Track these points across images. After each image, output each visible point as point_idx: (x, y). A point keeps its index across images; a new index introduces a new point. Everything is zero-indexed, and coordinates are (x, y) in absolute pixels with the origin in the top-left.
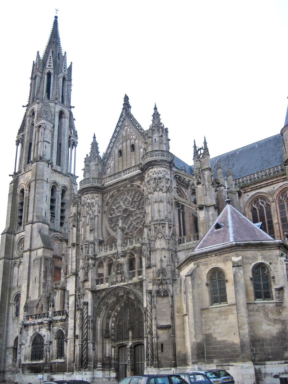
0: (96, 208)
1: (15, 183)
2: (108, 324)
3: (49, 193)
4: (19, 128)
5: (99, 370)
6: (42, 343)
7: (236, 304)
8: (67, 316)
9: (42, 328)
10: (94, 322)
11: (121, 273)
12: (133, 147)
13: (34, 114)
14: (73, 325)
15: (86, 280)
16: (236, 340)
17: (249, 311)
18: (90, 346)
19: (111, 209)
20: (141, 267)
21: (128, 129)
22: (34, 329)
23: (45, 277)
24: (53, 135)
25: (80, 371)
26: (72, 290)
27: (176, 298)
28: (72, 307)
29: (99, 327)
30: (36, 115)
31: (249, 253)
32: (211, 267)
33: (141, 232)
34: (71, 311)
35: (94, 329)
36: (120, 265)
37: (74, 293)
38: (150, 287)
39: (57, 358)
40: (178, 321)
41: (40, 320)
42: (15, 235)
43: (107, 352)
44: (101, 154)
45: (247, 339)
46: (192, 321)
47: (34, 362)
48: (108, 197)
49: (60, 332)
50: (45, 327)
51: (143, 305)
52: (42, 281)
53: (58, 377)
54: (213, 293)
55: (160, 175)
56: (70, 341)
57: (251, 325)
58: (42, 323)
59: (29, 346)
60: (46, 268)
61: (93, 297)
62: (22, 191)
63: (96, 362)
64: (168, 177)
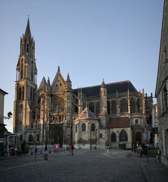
0: (50, 101)
1: (18, 85)
3: (30, 91)
4: (17, 64)
6: (32, 137)
7: (88, 132)
8: (40, 130)
10: (49, 132)
12: (61, 85)
13: (23, 60)
14: (42, 133)
15: (47, 121)
16: (87, 139)
17: (90, 133)
18: (48, 139)
19: (54, 101)
20: (63, 119)
21: (59, 78)
23: (31, 118)
24: (30, 70)
27: (73, 129)
29: (50, 134)
30: (24, 61)
31: (91, 121)
32: (83, 123)
33: (63, 110)
35: (49, 134)
36: (57, 118)
38: (66, 125)
40: (73, 134)
41: (31, 131)
42: (19, 103)
44: (51, 84)
45: (89, 139)
46: (78, 135)
47: (30, 142)
48: (53, 98)
49: (38, 134)
51: (63, 129)
52: (30, 119)
54: (82, 129)
55: (69, 95)
57: (90, 137)
60: (31, 115)
61: (49, 126)
62: (20, 88)
63: (50, 143)
64: (71, 96)
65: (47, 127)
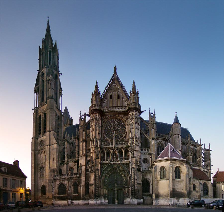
2: (105, 180)
5: (103, 199)
9: (64, 180)
11: (115, 157)
22: (59, 181)
25: (95, 199)
26: (84, 163)
28: (84, 171)
29: (102, 181)
34: (83, 173)
37: (85, 165)
39: (74, 194)
43: (104, 192)
50: (66, 180)
53: (76, 202)
56: (83, 187)
58: (64, 178)
59: (57, 189)
61: (101, 166)
65: (97, 168)
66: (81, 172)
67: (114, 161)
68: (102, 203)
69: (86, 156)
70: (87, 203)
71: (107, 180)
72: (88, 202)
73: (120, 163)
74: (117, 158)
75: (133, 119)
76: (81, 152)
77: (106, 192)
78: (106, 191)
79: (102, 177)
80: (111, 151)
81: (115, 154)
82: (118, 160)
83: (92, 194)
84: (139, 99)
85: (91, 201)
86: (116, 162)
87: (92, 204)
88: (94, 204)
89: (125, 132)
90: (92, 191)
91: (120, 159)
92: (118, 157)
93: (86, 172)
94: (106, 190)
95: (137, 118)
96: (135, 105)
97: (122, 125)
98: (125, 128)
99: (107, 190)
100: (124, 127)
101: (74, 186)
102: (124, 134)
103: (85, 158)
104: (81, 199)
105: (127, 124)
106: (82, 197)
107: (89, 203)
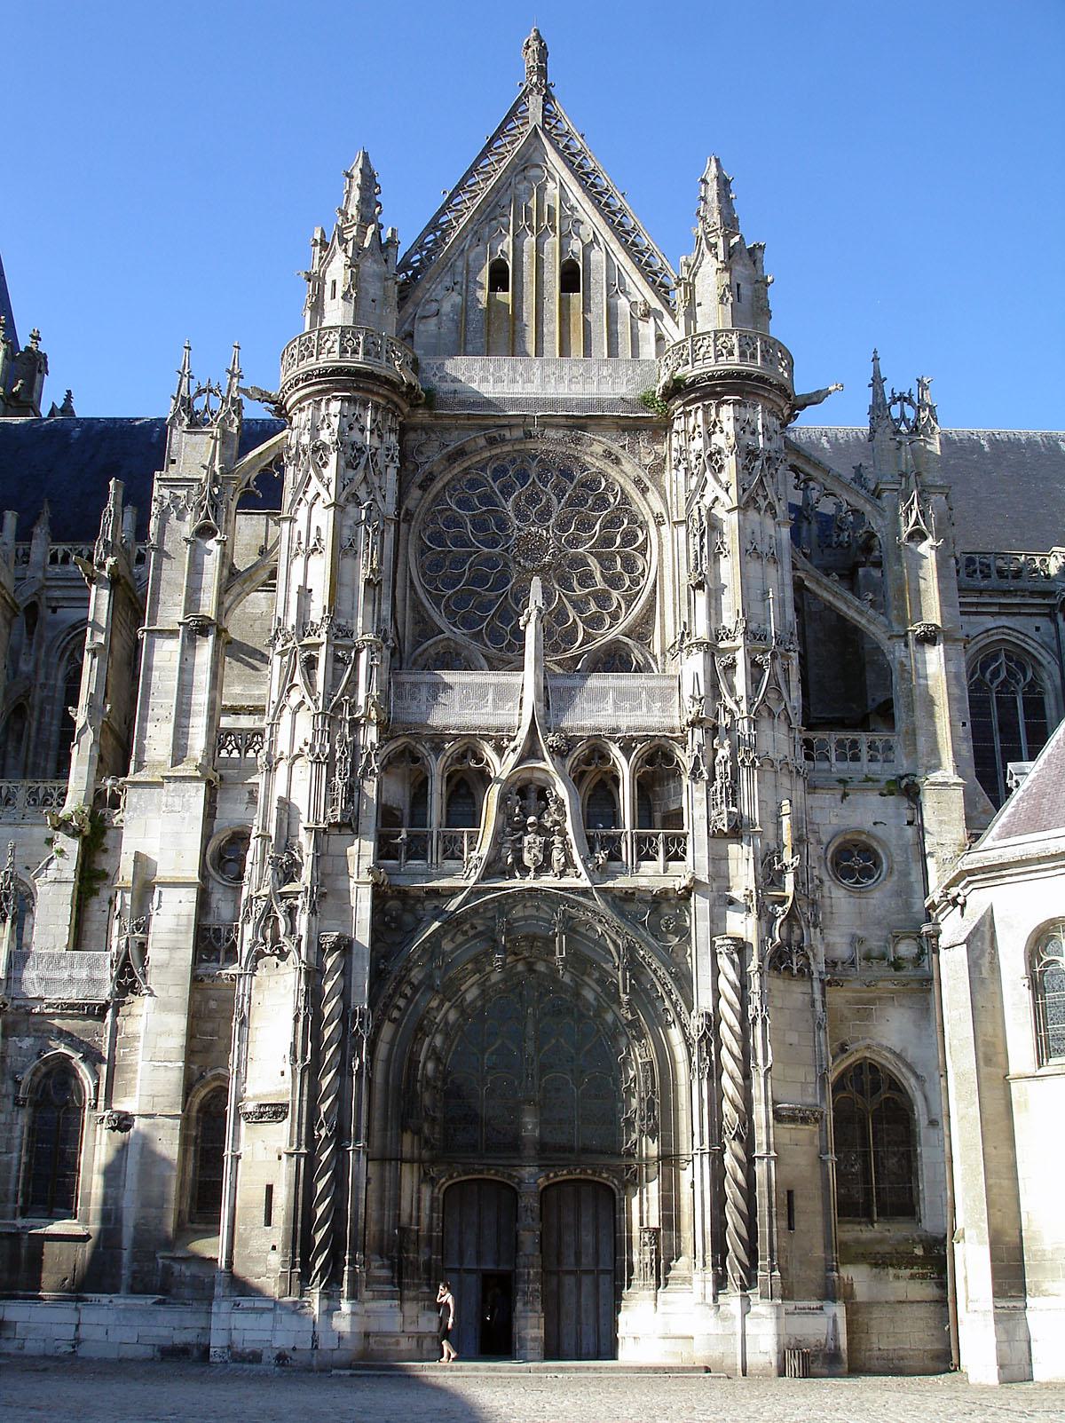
2: (413, 1063)
11: (541, 830)
26: (180, 854)
28: (173, 949)
29: (379, 1078)
37: (194, 876)
43: (405, 1204)
66: (143, 947)
67: (525, 871)
68: (372, 1340)
69: (209, 783)
70: (180, 1338)
71: (430, 1066)
72: (206, 1330)
73: (585, 892)
74: (563, 833)
75: (721, 467)
76: (157, 739)
77: (426, 1203)
78: (426, 1192)
79: (387, 1030)
80: (501, 767)
81: (533, 796)
82: (569, 862)
83: (268, 1222)
84: (772, 294)
85: (239, 1320)
86: (548, 881)
87: (255, 1357)
88: (281, 1358)
89: (635, 582)
90: (270, 1189)
91: (592, 850)
92: (569, 826)
93: (196, 960)
94: (426, 1178)
95: (757, 457)
96: (731, 353)
97: (612, 523)
98: (643, 549)
99: (433, 1182)
100: (630, 538)
101: (36, 1105)
102: (630, 601)
103: (196, 796)
104: (114, 1289)
105: (658, 507)
106: (134, 1258)
107: (217, 1341)
